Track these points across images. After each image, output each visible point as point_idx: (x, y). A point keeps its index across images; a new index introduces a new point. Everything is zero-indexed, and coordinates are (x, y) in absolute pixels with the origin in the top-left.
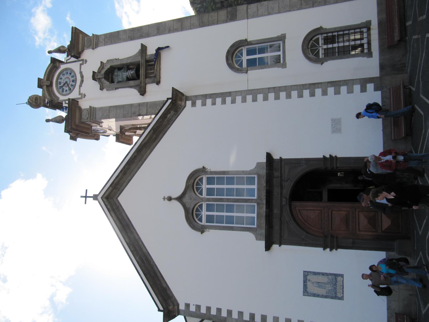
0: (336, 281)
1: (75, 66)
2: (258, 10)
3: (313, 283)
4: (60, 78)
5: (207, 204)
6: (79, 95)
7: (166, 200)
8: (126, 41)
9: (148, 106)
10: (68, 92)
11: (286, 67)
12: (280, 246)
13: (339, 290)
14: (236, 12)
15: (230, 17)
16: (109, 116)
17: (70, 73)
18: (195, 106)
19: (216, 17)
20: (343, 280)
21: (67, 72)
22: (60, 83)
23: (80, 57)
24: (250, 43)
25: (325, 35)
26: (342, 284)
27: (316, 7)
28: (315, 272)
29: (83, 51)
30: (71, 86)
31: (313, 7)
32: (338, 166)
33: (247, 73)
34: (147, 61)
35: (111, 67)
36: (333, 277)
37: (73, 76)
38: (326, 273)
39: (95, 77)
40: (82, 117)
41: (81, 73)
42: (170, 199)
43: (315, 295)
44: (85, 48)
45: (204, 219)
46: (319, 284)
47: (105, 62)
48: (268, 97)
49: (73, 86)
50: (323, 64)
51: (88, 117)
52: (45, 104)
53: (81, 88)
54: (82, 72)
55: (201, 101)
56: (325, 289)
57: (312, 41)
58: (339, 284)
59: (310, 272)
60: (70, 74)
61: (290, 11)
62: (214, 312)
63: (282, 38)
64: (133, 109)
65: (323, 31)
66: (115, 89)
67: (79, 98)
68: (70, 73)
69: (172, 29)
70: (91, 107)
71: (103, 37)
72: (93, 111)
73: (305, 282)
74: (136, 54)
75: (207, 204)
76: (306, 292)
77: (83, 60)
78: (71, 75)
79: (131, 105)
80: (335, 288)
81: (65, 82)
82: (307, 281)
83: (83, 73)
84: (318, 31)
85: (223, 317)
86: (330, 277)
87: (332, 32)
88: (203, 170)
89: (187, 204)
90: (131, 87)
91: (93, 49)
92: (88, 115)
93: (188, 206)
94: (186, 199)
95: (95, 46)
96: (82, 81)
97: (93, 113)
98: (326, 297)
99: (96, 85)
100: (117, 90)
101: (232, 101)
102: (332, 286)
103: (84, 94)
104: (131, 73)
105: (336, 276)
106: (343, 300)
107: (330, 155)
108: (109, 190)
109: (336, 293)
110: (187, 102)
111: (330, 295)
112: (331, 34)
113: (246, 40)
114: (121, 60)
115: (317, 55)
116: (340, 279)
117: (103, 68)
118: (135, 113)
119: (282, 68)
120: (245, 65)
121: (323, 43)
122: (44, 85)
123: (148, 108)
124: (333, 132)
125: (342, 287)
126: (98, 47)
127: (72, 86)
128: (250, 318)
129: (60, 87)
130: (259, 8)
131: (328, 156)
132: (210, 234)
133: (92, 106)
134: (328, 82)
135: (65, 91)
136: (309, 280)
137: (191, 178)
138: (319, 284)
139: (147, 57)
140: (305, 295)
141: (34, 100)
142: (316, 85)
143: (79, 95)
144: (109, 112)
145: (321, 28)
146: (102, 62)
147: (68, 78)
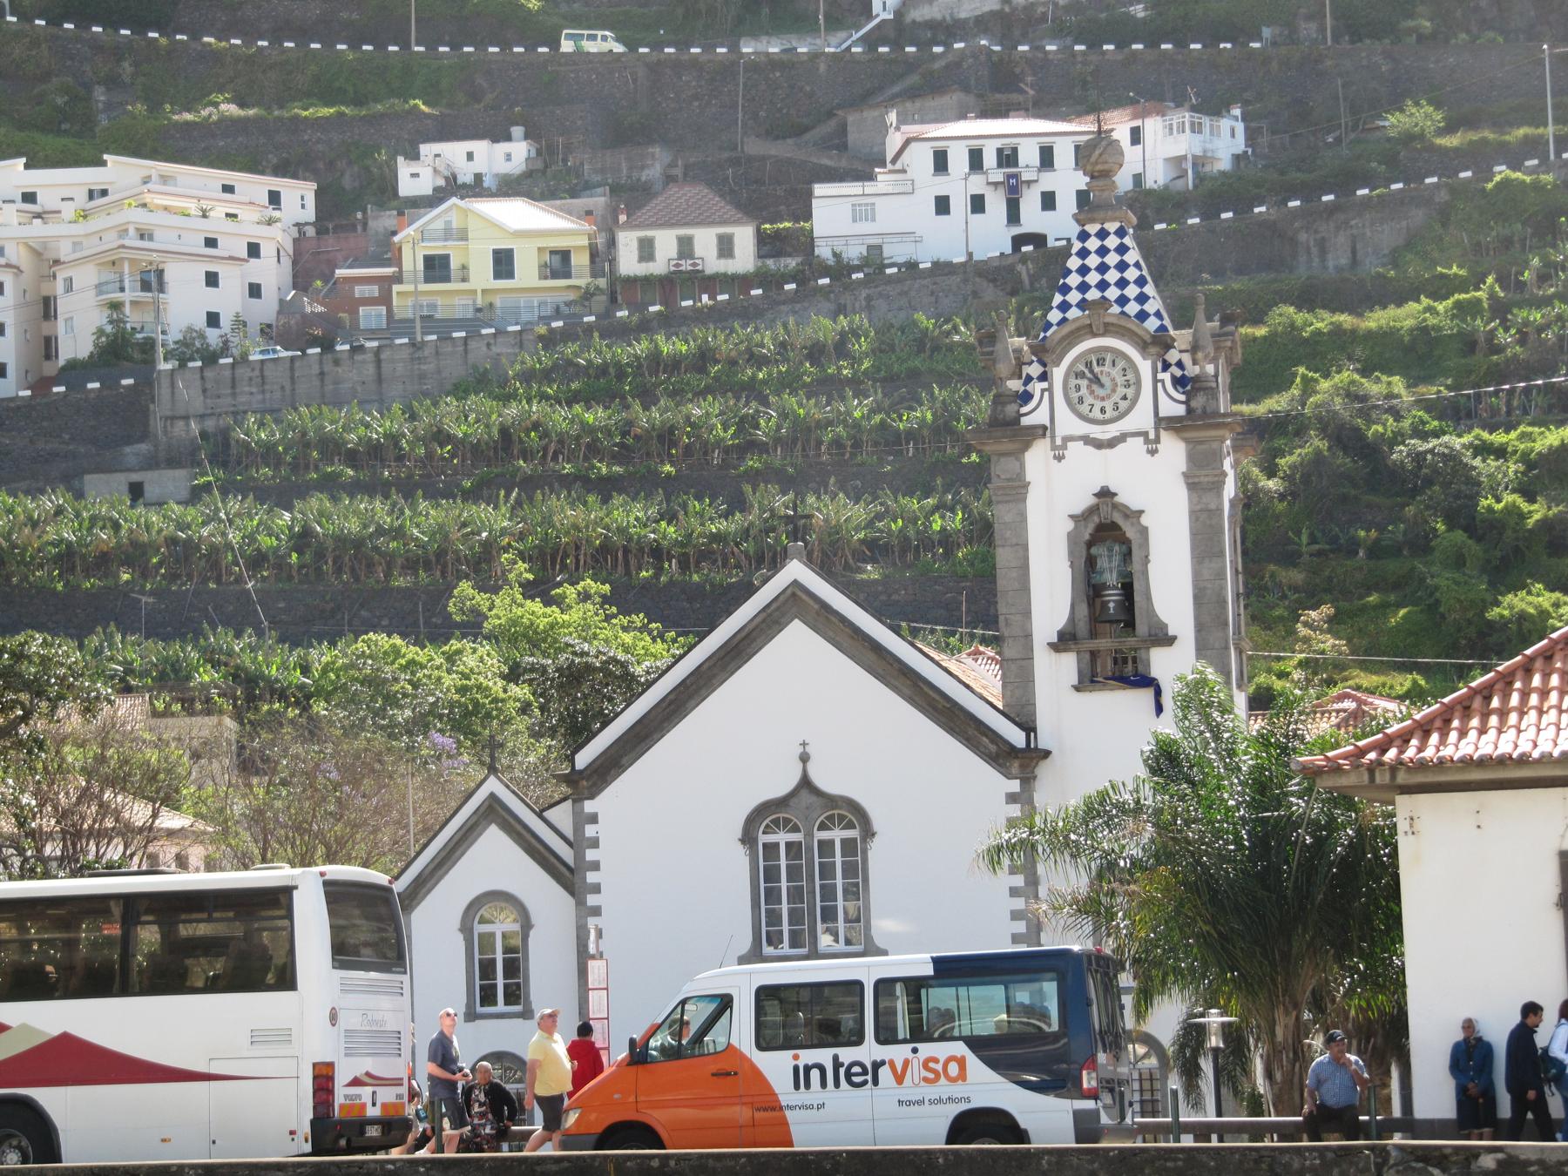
1: (1140, 416)
7: (801, 749)
39: (1105, 494)
40: (1002, 459)
41: (1122, 438)
42: (805, 758)
45: (771, 838)
47: (1144, 520)
62: (591, 877)
64: (1018, 617)
67: (1053, 437)
70: (1026, 485)
71: (1213, 506)
77: (1157, 440)
79: (1027, 613)
81: (1104, 379)
88: (868, 833)
93: (793, 802)
94: (806, 798)
96: (1099, 445)
99: (1083, 501)
103: (1063, 457)
114: (1145, 573)
132: (739, 860)
135: (1079, 381)
141: (1099, 167)
147: (1114, 391)
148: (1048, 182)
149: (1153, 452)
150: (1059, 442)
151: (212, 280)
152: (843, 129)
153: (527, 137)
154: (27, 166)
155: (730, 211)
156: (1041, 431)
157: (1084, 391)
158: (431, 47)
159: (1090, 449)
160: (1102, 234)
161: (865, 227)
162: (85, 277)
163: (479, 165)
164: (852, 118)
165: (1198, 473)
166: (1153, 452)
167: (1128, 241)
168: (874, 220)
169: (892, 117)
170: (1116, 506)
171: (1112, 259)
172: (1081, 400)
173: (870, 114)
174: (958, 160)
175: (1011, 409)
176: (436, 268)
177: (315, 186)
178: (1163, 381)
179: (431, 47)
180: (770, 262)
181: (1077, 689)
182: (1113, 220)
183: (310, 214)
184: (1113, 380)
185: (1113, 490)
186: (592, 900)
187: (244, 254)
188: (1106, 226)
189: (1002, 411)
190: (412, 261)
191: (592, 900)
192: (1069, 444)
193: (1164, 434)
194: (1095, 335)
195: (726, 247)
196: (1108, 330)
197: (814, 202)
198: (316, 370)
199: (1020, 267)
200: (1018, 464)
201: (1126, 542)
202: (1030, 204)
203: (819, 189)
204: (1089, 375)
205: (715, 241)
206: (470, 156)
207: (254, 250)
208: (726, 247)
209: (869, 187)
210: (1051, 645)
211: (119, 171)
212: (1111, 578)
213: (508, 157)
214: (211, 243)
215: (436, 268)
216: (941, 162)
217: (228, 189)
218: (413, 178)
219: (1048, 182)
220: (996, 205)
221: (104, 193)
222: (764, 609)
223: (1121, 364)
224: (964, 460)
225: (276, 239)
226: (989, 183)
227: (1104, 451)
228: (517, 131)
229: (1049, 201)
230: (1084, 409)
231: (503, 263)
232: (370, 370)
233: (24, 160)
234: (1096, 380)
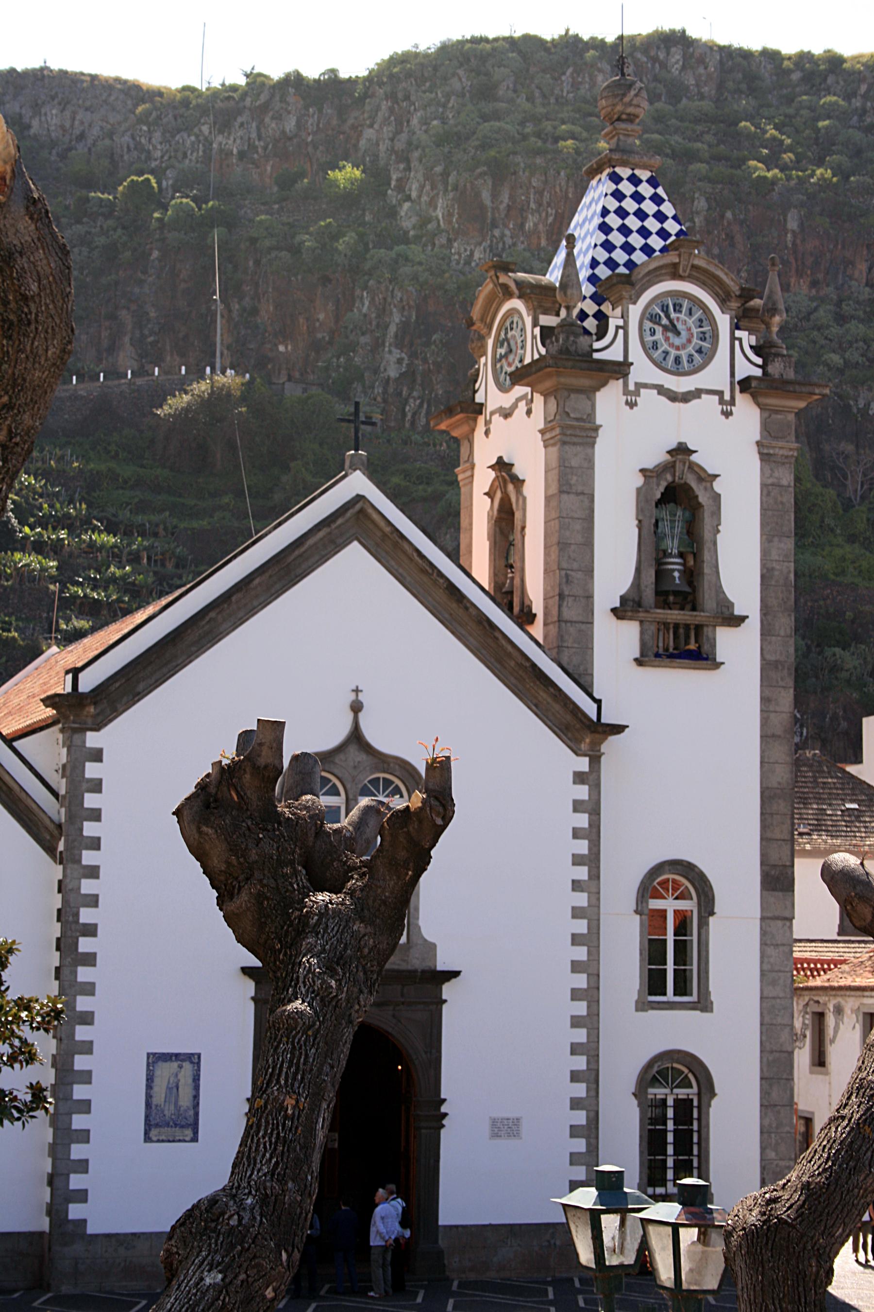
0: (182, 1127)
2: (777, 945)
3: (177, 1075)
4: (694, 309)
5: (339, 808)
6: (636, 384)
7: (352, 696)
8: (761, 560)
9: (583, 627)
10: (649, 339)
11: (637, 1010)
12: (253, 998)
13: (166, 1132)
14: (782, 890)
15: (773, 873)
16: (568, 493)
17: (701, 348)
18: (574, 783)
19: (778, 836)
20: (185, 1141)
21: (707, 336)
22: (677, 308)
23: (742, 391)
24: (703, 924)
25: (695, 1103)
26: (177, 1138)
27: (761, 1085)
28: (199, 1080)
29: (758, 405)
30: (664, 352)
31: (762, 1079)
32: (423, 1131)
33: (636, 912)
34: (699, 628)
35: (699, 506)
36: (191, 1120)
37: (692, 361)
38: (198, 1104)
39: (682, 451)
40: (572, 396)
41: (697, 393)
42: (356, 708)
43: (150, 1080)
44: (766, 414)
46: (174, 1088)
47: (717, 486)
48: (579, 972)
49: (664, 359)
50: (633, 1098)
51: (572, 415)
52: (614, 164)
53: (655, 392)
54: (699, 397)
55: (586, 798)
56: (165, 1101)
57: (686, 1071)
58: (178, 1133)
59: (199, 1070)
60: (697, 347)
61: (762, 1024)
62: (90, 829)
63: (704, 1005)
64: (579, 575)
65: (704, 1099)
66: (640, 518)
67: (626, 385)
68: (703, 349)
69: (771, 708)
70: (596, 429)
72: (587, 437)
73: (177, 1056)
74: (724, 592)
75: (339, 808)
76: (155, 1059)
77: (732, 402)
78: (697, 352)
80: (168, 1125)
81: (679, 326)
82: (179, 1062)
83: (695, 402)
84: (707, 1088)
85: (80, 855)
86: (191, 1113)
87: (699, 1119)
89: (342, 756)
90: (638, 570)
91: (758, 443)
92: (578, 416)
93: (339, 759)
94: (354, 754)
95: (765, 451)
96: (673, 397)
97: (579, 436)
98: (148, 1105)
99: (656, 457)
100: (636, 522)
101: (579, 881)
102: (173, 1117)
103: (636, 404)
104: (674, 570)
105: (195, 1126)
106: (145, 1141)
107: (446, 1115)
108: (382, 524)
109: (157, 1125)
110: (587, 759)
111: (153, 1114)
112: (695, 1115)
113: (712, 913)
114: (715, 543)
115: (654, 1081)
116: (186, 1136)
117: (700, 479)
118: (567, 582)
119: (637, 1002)
120: (655, 904)
121: (680, 1097)
122: (679, 256)
123: (577, 625)
124: (494, 1122)
125: (171, 1139)
126: (762, 460)
127: (664, 355)
128: (85, 925)
129: (667, 306)
130: (781, 948)
131: (443, 1109)
133: (600, 431)
134: (597, 1113)
136: (181, 1067)
137: (407, 771)
138: (174, 1088)
139: (710, 629)
140: (148, 1058)
141: (630, 110)
142: (594, 1086)
143: (636, 384)
144: (579, 491)
145: (713, 1094)
147: (689, 341)
149: (727, 414)
150: (632, 387)
156: (621, 369)
157: (659, 336)
159: (663, 399)
165: (774, 443)
166: (727, 414)
167: (660, 191)
170: (694, 468)
171: (649, 207)
178: (740, 340)
181: (639, 662)
184: (689, 329)
186: (88, 857)
189: (575, 342)
191: (88, 857)
192: (642, 391)
193: (738, 396)
194: (676, 276)
200: (589, 403)
201: (693, 507)
204: (665, 321)
210: (614, 610)
212: (672, 545)
223: (698, 314)
227: (677, 404)
230: (657, 354)
234: (672, 328)
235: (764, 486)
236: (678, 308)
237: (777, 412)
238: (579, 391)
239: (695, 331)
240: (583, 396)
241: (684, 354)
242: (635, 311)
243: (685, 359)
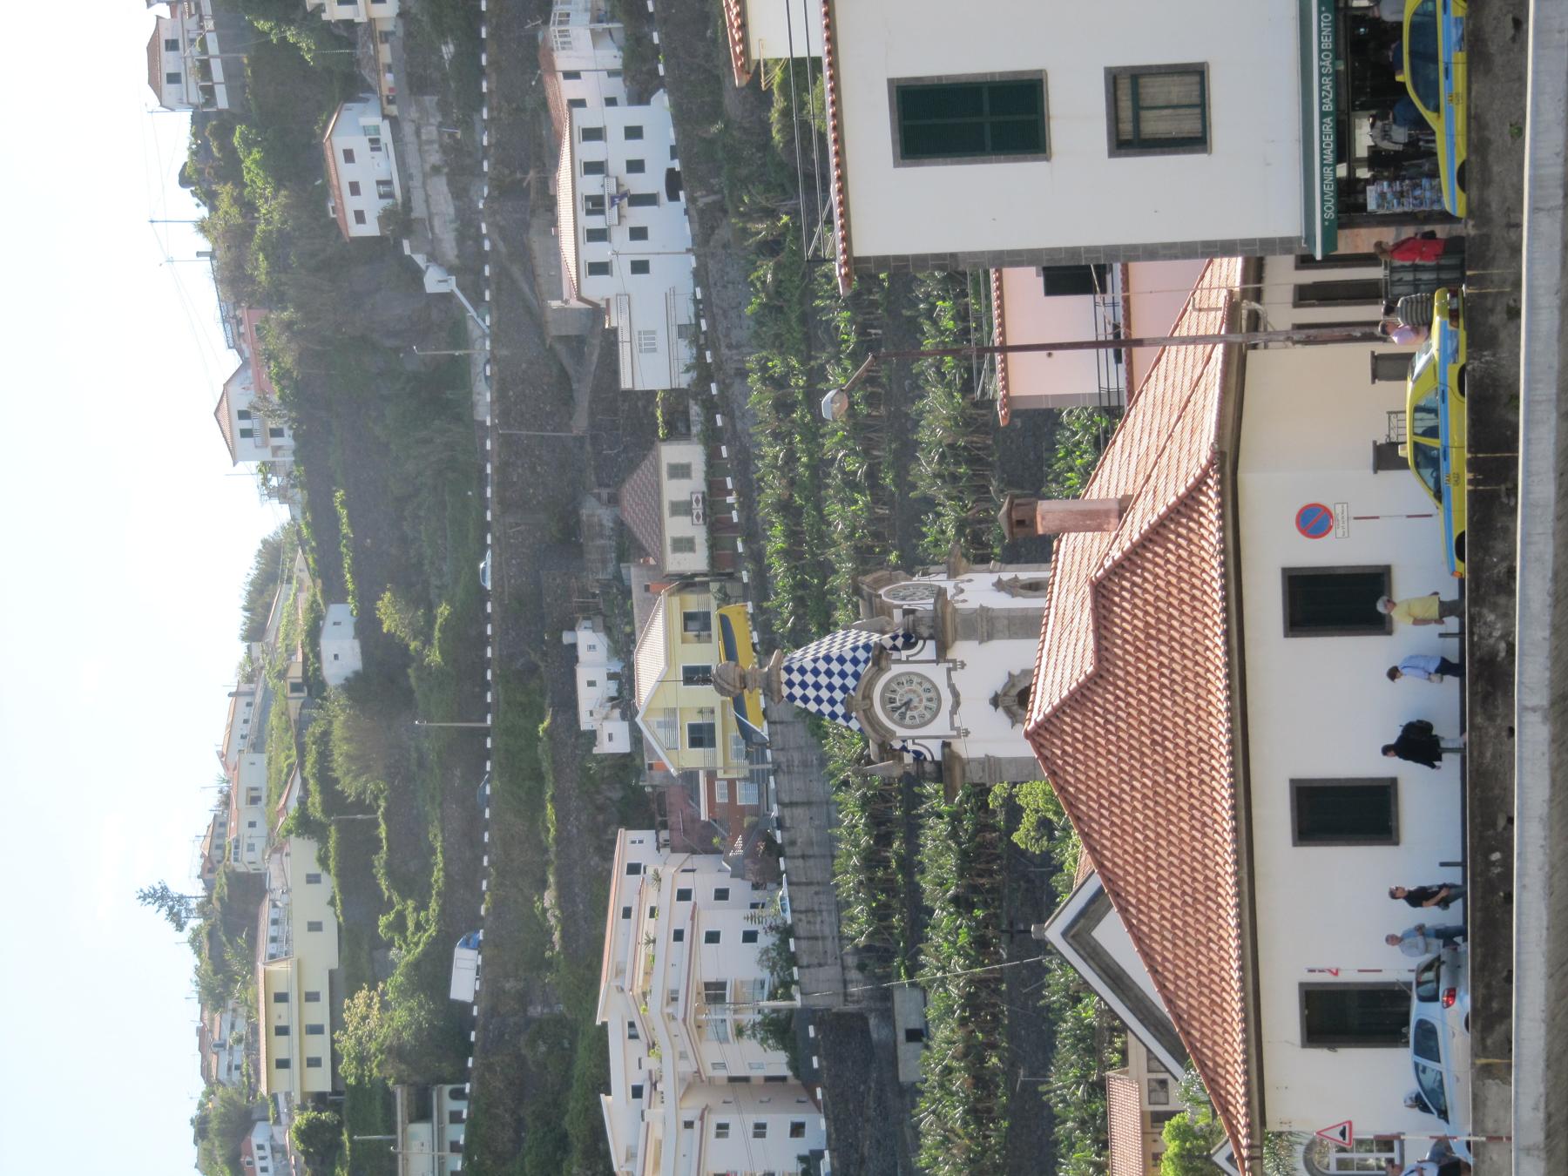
1: (937, 674)
39: (995, 701)
41: (952, 687)
47: (1016, 672)
67: (953, 737)
71: (1006, 622)
77: (954, 661)
81: (905, 700)
83: (958, 687)
96: (957, 703)
117: (1013, 685)
141: (738, 685)
146: (1010, 675)
147: (915, 692)
148: (617, 166)
149: (963, 665)
150: (955, 733)
151: (713, 937)
152: (561, 338)
153: (572, 629)
154: (608, 1093)
155: (646, 465)
157: (915, 713)
158: (487, 708)
159: (961, 709)
160: (790, 684)
161: (661, 341)
162: (711, 1052)
163: (600, 675)
164: (553, 331)
166: (963, 665)
168: (654, 332)
169: (555, 304)
172: (922, 716)
173: (549, 317)
174: (598, 252)
175: (928, 767)
176: (701, 736)
177: (621, 831)
179: (487, 708)
180: (695, 430)
182: (779, 675)
183: (648, 836)
185: (992, 695)
187: (687, 905)
188: (784, 680)
190: (695, 758)
194: (872, 705)
195: (681, 471)
196: (867, 697)
197: (639, 387)
198: (800, 862)
199: (700, 204)
202: (639, 184)
203: (626, 383)
204: (903, 709)
205: (675, 482)
206: (591, 684)
207: (684, 895)
208: (681, 471)
209: (623, 336)
211: (610, 1010)
213: (592, 648)
214: (678, 935)
215: (701, 736)
216: (599, 269)
217: (627, 913)
218: (613, 739)
219: (617, 166)
220: (639, 216)
221: (632, 1025)
222: (1085, 960)
224: (886, 284)
225: (671, 869)
226: (619, 223)
228: (567, 638)
229: (636, 166)
231: (695, 675)
232: (799, 812)
233: (602, 1096)
234: (907, 704)
235: (1010, 637)
236: (892, 701)
237: (956, 630)
238: (964, 771)
239: (907, 687)
240: (967, 768)
241: (925, 696)
242: (901, 732)
243: (929, 695)
